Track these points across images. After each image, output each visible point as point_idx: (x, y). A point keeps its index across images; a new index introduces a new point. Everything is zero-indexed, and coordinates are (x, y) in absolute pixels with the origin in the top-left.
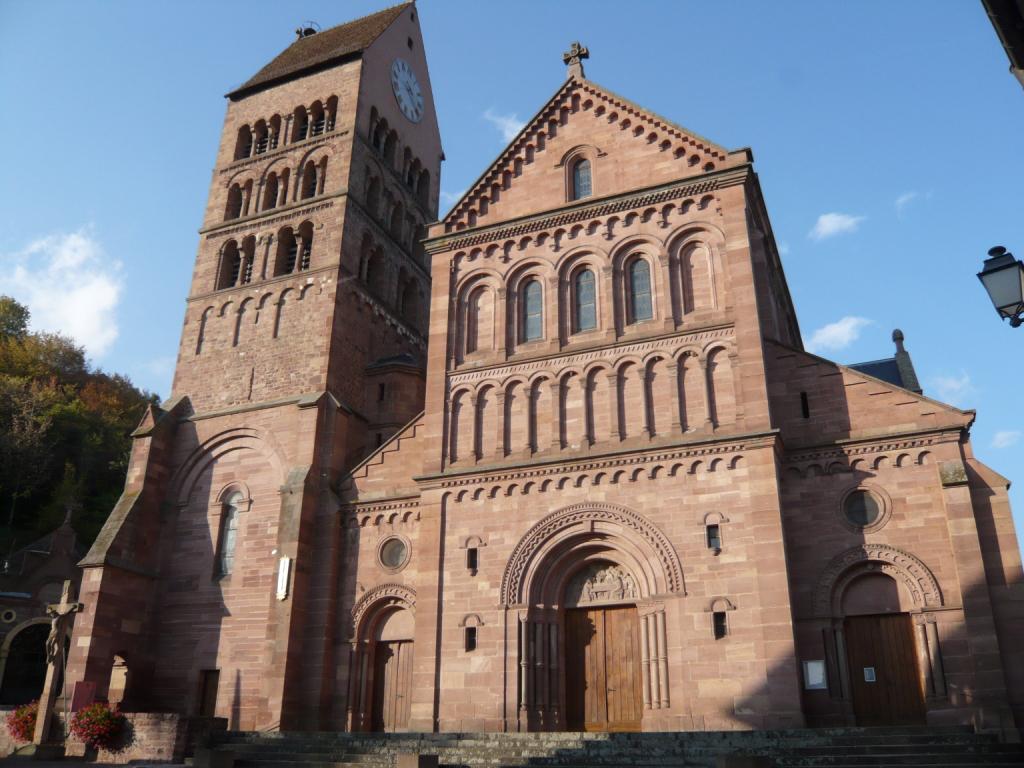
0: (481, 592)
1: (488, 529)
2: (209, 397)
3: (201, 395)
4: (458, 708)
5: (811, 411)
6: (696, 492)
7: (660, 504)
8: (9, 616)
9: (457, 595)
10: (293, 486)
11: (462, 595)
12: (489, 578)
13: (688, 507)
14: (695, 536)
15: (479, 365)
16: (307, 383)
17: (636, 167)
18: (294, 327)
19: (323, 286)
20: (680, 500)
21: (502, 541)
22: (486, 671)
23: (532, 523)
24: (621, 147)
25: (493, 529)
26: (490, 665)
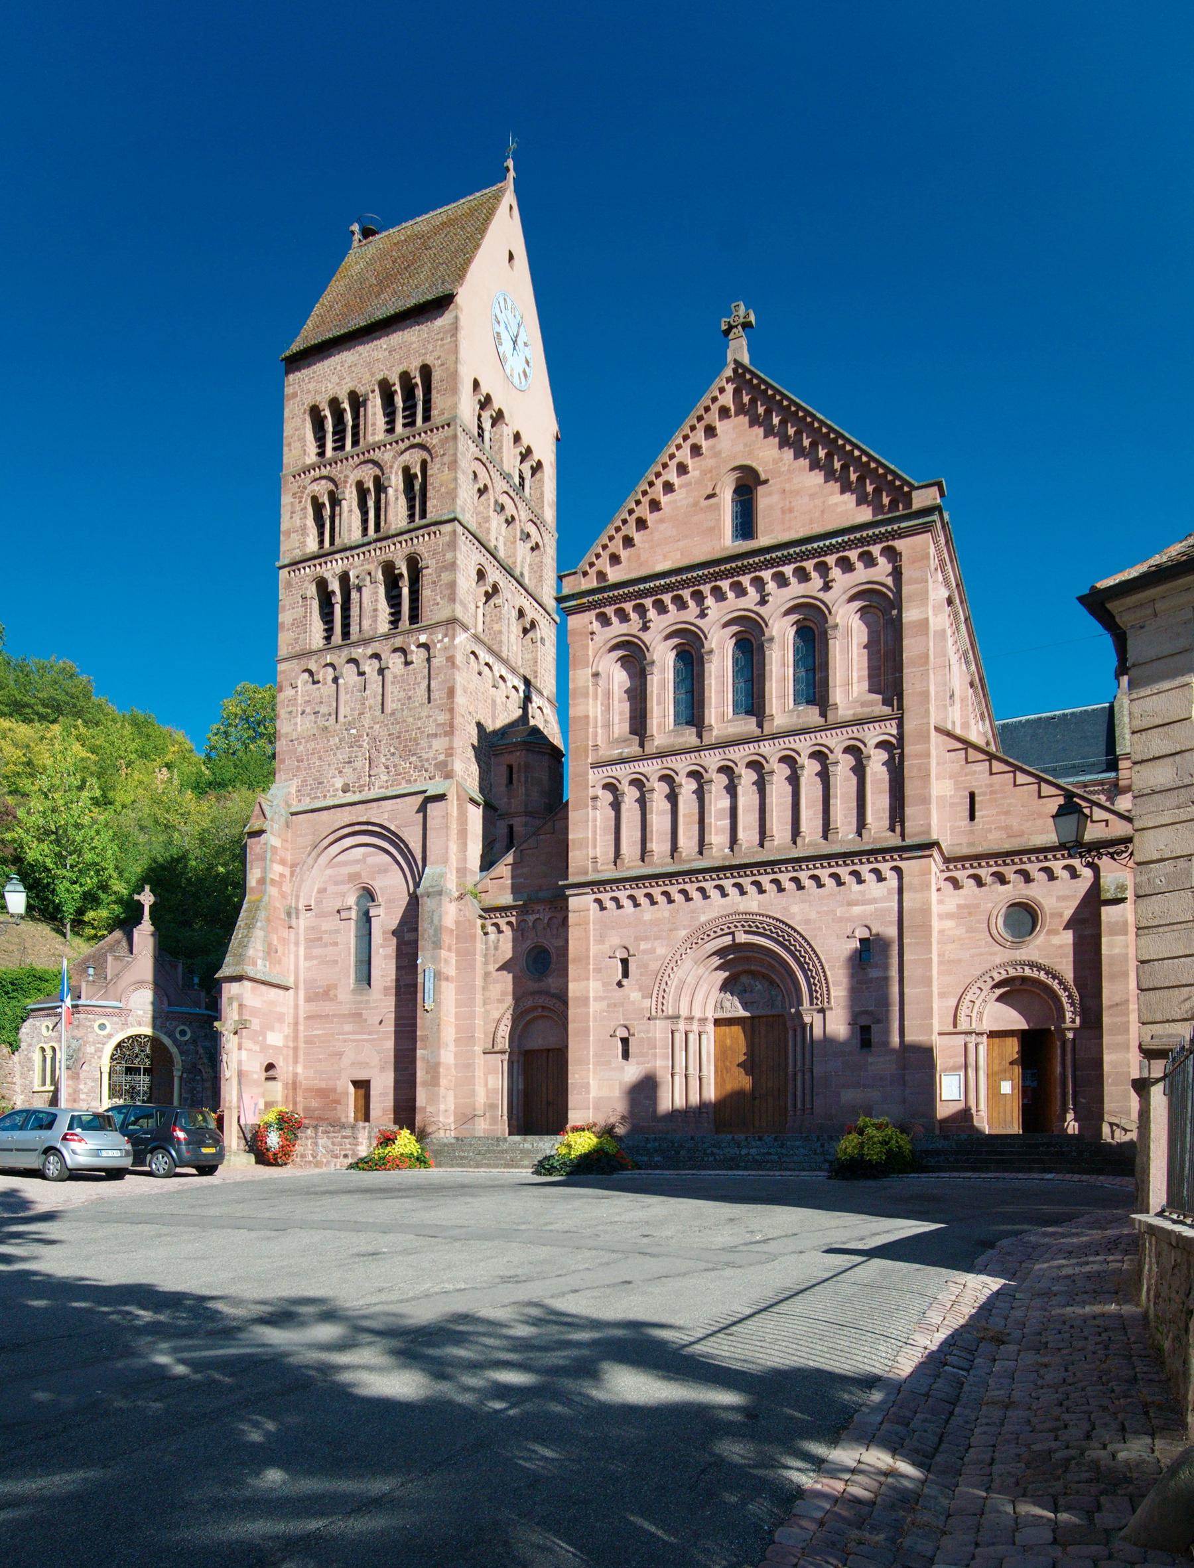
0: (633, 1003)
2: (320, 783)
3: (310, 781)
5: (977, 814)
6: (851, 904)
7: (813, 915)
8: (102, 1027)
9: (609, 1006)
10: (430, 890)
12: (640, 989)
15: (625, 755)
16: (432, 768)
17: (806, 499)
18: (410, 698)
19: (439, 645)
20: (833, 912)
21: (653, 951)
24: (789, 471)
25: (645, 939)
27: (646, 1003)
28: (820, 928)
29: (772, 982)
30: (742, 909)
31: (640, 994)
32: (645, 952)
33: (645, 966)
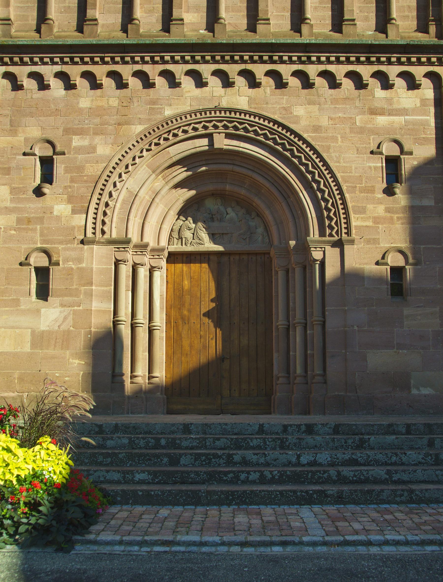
0: (58, 218)
1: (69, 131)
4: (21, 379)
6: (374, 112)
7: (324, 122)
11: (29, 221)
12: (70, 200)
13: (362, 130)
14: (370, 167)
20: (352, 120)
21: (92, 149)
22: (63, 327)
23: (139, 129)
25: (81, 132)
26: (70, 320)
27: (79, 220)
28: (334, 139)
29: (250, 209)
30: (224, 104)
31: (69, 207)
32: (79, 150)
33: (80, 169)
